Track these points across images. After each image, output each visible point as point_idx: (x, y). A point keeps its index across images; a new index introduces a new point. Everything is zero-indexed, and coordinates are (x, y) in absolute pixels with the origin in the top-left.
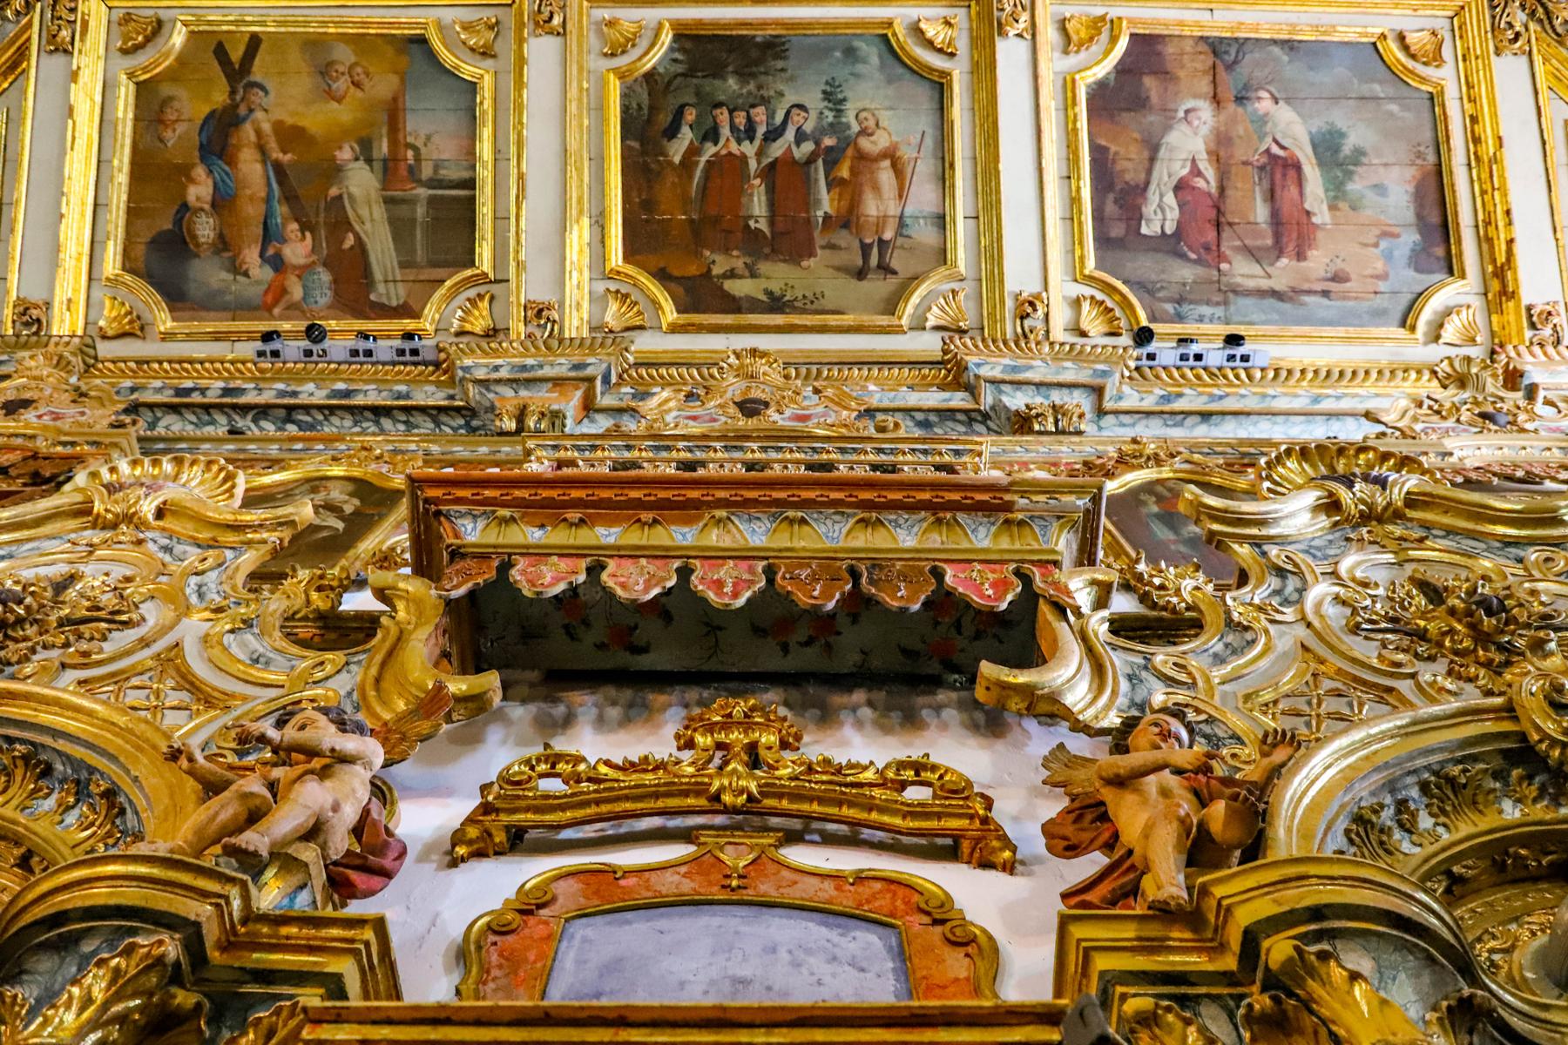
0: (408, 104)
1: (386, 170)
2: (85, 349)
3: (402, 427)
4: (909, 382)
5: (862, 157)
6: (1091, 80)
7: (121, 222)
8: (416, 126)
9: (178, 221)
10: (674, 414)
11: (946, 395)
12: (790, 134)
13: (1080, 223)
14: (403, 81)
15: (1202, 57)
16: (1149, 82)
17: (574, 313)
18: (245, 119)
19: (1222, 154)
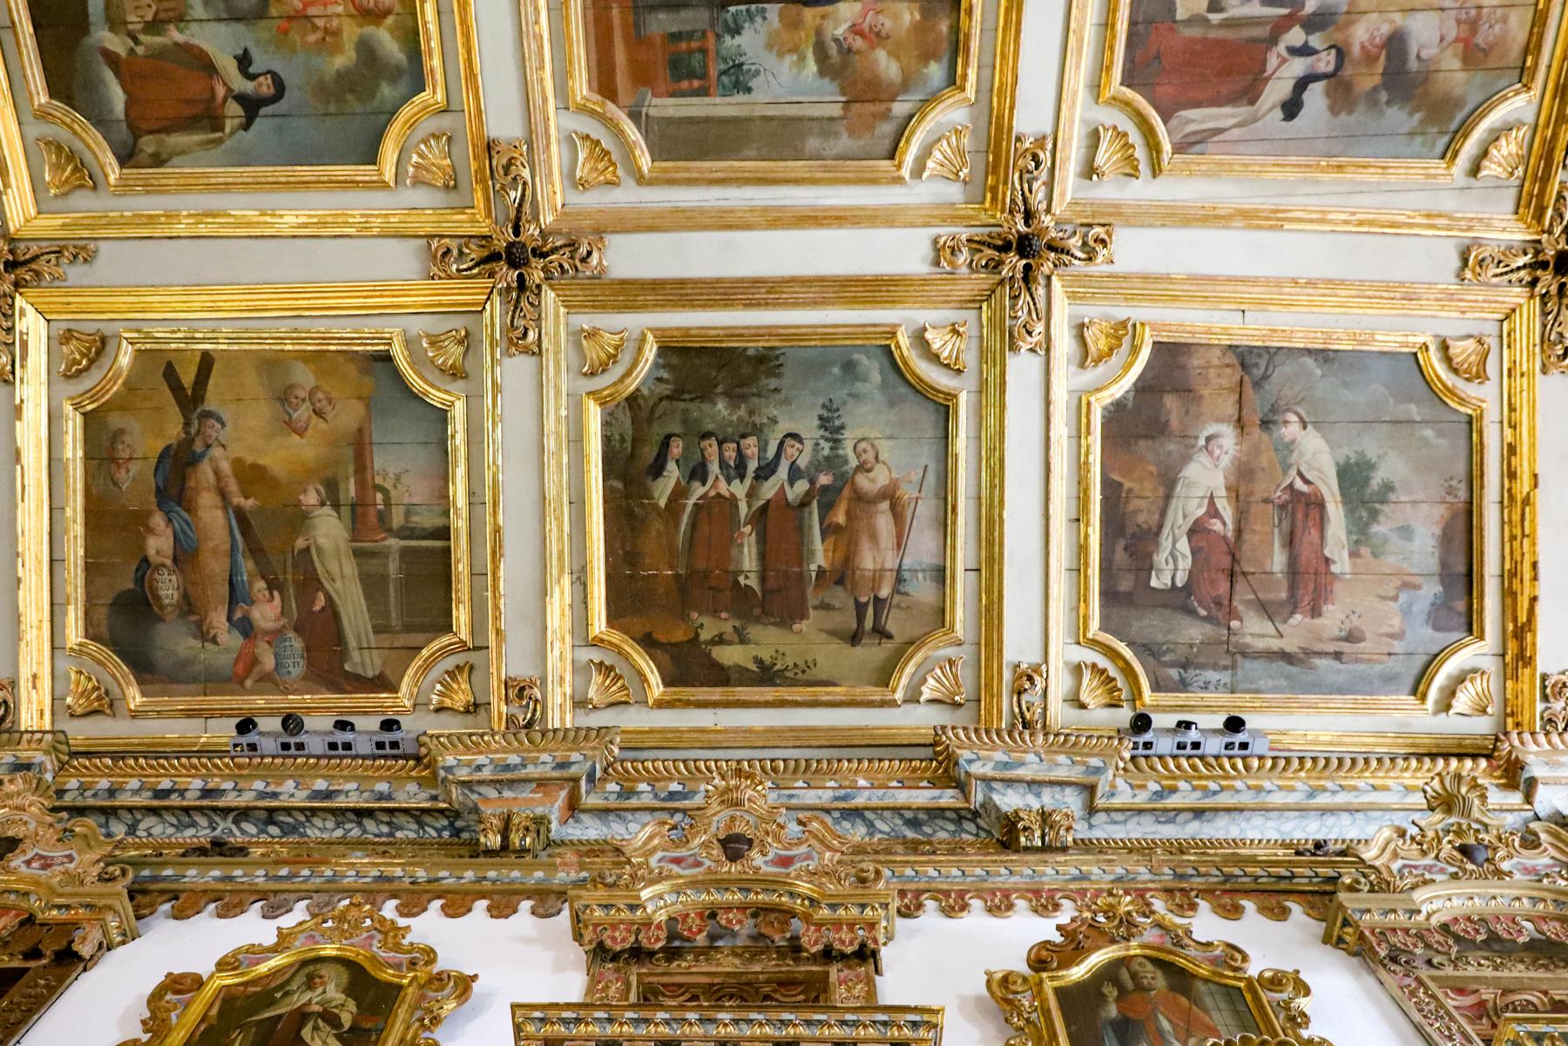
0: (375, 438)
1: (354, 517)
2: (59, 746)
3: (385, 829)
4: (899, 775)
5: (860, 498)
6: (1109, 401)
7: (80, 582)
8: (384, 463)
9: (140, 580)
10: (659, 855)
11: (936, 792)
12: (783, 472)
13: (1086, 576)
14: (367, 407)
15: (1229, 370)
16: (1171, 402)
17: (558, 689)
18: (203, 455)
19: (1242, 490)
